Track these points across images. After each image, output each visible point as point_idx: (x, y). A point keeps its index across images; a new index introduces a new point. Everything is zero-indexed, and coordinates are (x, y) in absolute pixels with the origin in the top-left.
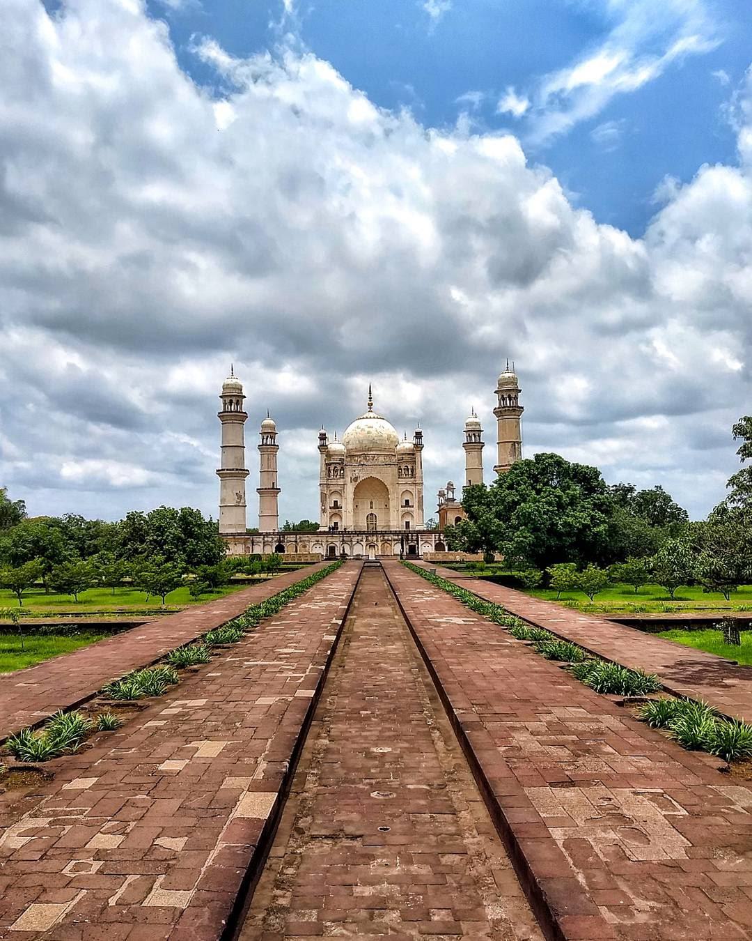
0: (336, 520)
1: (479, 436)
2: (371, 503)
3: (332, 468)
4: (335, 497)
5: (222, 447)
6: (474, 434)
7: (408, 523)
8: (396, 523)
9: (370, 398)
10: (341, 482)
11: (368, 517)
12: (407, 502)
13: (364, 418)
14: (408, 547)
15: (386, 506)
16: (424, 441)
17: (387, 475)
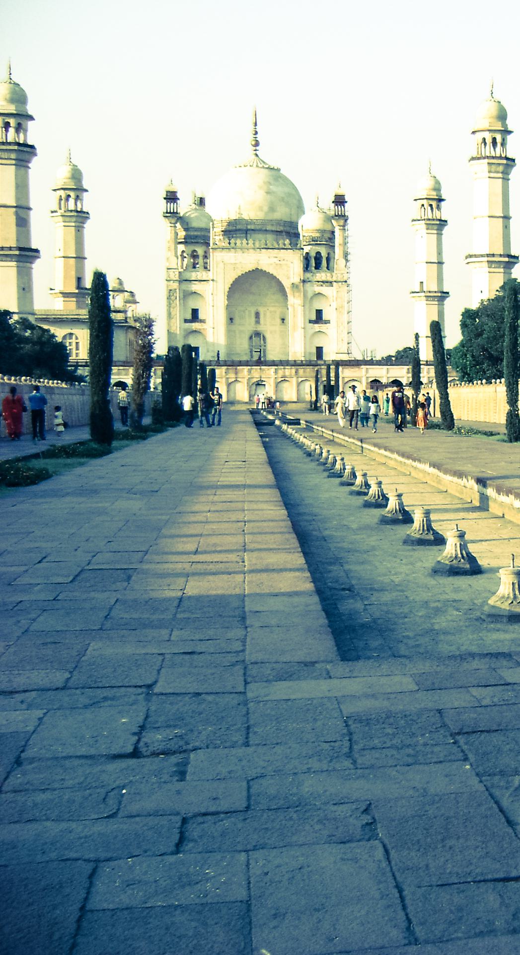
1: (438, 208)
4: (193, 304)
6: (431, 205)
11: (251, 338)
15: (283, 320)
16: (349, 209)
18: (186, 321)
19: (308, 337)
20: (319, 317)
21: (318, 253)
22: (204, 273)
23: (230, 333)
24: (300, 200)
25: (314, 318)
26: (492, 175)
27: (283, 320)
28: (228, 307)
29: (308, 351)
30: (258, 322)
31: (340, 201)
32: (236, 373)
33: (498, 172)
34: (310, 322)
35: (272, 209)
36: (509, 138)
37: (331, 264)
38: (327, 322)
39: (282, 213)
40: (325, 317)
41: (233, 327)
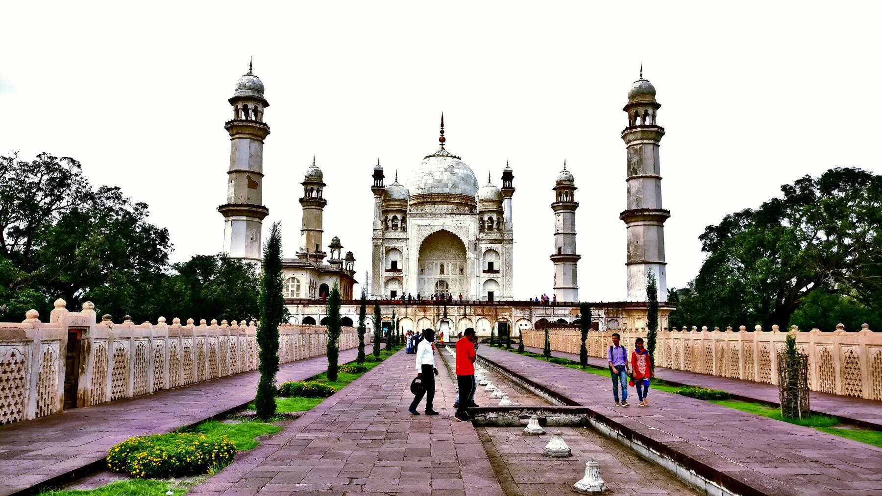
0: (393, 286)
1: (572, 195)
2: (442, 267)
3: (391, 216)
4: (393, 257)
5: (229, 173)
6: (566, 194)
7: (491, 294)
8: (475, 290)
9: (442, 132)
10: (402, 235)
11: (437, 284)
12: (491, 265)
13: (434, 156)
14: (496, 325)
15: (462, 270)
16: (515, 183)
17: (466, 228)
18: (387, 271)
19: (482, 283)
20: (491, 269)
21: (490, 219)
22: (402, 233)
23: (420, 279)
24: (475, 181)
25: (486, 268)
26: (645, 141)
27: (462, 270)
28: (419, 260)
29: (481, 294)
30: (442, 271)
31: (508, 176)
32: (425, 311)
33: (649, 139)
34: (484, 272)
35: (455, 186)
36: (659, 112)
37: (501, 227)
38: (498, 272)
39: (462, 189)
40: (495, 268)
41: (423, 276)
